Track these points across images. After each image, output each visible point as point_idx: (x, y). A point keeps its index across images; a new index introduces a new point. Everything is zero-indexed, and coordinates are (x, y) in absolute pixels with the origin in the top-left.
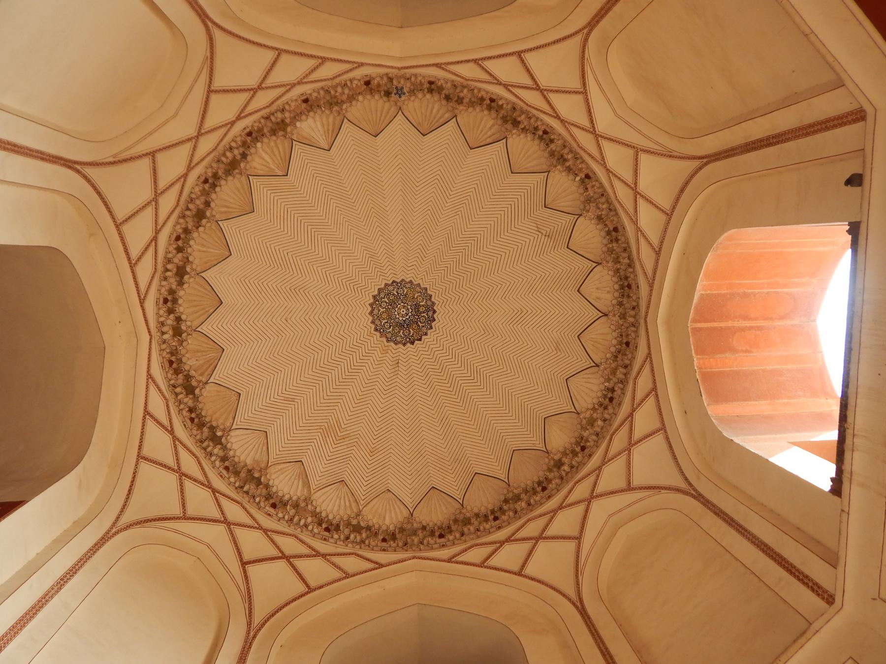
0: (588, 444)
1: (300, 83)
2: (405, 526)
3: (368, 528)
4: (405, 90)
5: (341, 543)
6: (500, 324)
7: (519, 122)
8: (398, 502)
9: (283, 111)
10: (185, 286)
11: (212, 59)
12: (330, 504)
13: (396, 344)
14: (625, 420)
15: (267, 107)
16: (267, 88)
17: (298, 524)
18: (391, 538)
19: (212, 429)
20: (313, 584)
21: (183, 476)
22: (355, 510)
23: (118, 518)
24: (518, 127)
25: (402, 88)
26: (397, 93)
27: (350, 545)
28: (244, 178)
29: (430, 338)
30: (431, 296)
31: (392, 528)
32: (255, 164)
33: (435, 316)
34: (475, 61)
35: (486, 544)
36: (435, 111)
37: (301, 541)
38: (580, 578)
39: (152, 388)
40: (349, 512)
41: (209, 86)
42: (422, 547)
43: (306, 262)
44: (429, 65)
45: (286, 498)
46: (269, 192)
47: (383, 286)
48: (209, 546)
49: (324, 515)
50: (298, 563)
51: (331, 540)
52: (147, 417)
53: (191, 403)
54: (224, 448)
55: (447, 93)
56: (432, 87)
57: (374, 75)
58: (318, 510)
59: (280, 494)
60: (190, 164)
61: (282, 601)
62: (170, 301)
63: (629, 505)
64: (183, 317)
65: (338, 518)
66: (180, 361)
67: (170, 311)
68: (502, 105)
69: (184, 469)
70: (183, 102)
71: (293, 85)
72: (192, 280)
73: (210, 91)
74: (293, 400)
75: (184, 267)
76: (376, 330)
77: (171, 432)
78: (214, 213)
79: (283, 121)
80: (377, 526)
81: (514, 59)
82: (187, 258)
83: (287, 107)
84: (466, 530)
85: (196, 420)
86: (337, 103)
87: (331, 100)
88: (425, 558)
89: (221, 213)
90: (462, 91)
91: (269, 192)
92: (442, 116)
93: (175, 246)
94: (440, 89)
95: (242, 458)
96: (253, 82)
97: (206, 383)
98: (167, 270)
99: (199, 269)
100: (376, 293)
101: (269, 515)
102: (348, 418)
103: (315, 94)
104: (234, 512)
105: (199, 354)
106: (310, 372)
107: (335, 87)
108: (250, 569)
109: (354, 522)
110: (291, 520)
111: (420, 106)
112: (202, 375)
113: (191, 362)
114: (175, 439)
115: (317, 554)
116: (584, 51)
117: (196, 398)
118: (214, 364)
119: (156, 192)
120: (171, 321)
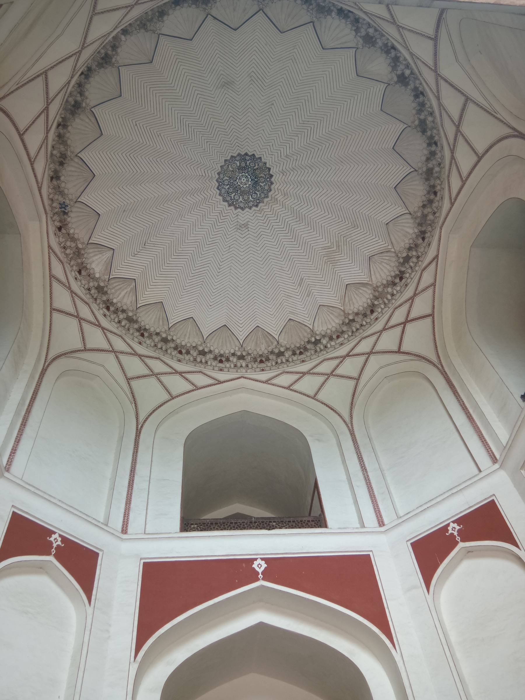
0: (389, 44)
1: (69, 288)
2: (417, 221)
3: (410, 249)
4: (61, 200)
5: (413, 274)
6: (263, 98)
8: (399, 219)
9: (89, 289)
10: (212, 349)
11: (65, 354)
12: (384, 271)
13: (271, 190)
14: (370, 18)
15: (89, 306)
16: (77, 311)
17: (389, 300)
18: (422, 235)
19: (309, 342)
20: (429, 311)
21: (332, 374)
22: (393, 255)
23: (344, 421)
25: (60, 204)
26: (64, 208)
27: (417, 268)
28: (138, 311)
29: (268, 160)
30: (232, 157)
31: (416, 231)
32: (128, 303)
33: (250, 154)
34: (32, 164)
35: (450, 169)
36: (73, 169)
37: (400, 305)
38: (498, 116)
39: (274, 381)
40: (394, 259)
41: (82, 350)
42: (437, 215)
43: (199, 259)
44: (41, 196)
45: (369, 301)
46: (148, 290)
47: (221, 198)
48: (381, 368)
49: (389, 278)
50: (412, 316)
51: (409, 280)
52: (291, 388)
53: (290, 353)
54: (324, 336)
55: (58, 164)
56: (55, 177)
57: (54, 228)
58: (385, 282)
59: (365, 305)
60: (133, 354)
61: (432, 337)
62: (221, 359)
63: (452, 43)
64: (232, 351)
65: (395, 269)
66: (261, 356)
67: (228, 360)
68: (62, 118)
69: (329, 371)
70: (94, 363)
71: (72, 292)
72: (208, 345)
73: (85, 350)
74: (302, 279)
75: (199, 351)
76: (257, 206)
77: (304, 374)
78: (163, 330)
79: (96, 288)
80: (411, 241)
81: (25, 137)
82: (194, 347)
83: (86, 286)
84: (436, 175)
85: (302, 350)
86: (79, 253)
87: (76, 256)
88: (446, 218)
89: (163, 324)
90: (55, 156)
91: (148, 290)
92: (77, 163)
93: (186, 355)
94: (56, 172)
95: (334, 325)
96: (75, 322)
97: (278, 343)
98: (201, 362)
99: (201, 340)
100: (226, 204)
101: (377, 319)
102: (324, 240)
103: (75, 268)
104: (365, 346)
105: (258, 342)
106: (283, 263)
107: (66, 255)
108: (403, 349)
109: (401, 260)
110: (385, 304)
111: (71, 184)
112: (272, 343)
113: (263, 349)
114: (308, 373)
115: (412, 299)
116: (12, 92)
117: (287, 349)
118: (266, 333)
119: (151, 375)
120: (235, 360)
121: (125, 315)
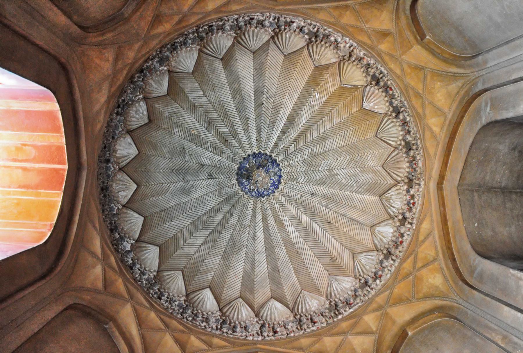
7: (178, 306)
13: (266, 154)
24: (179, 303)
53: (408, 137)
54: (391, 104)
93: (404, 238)
121: (359, 290)
